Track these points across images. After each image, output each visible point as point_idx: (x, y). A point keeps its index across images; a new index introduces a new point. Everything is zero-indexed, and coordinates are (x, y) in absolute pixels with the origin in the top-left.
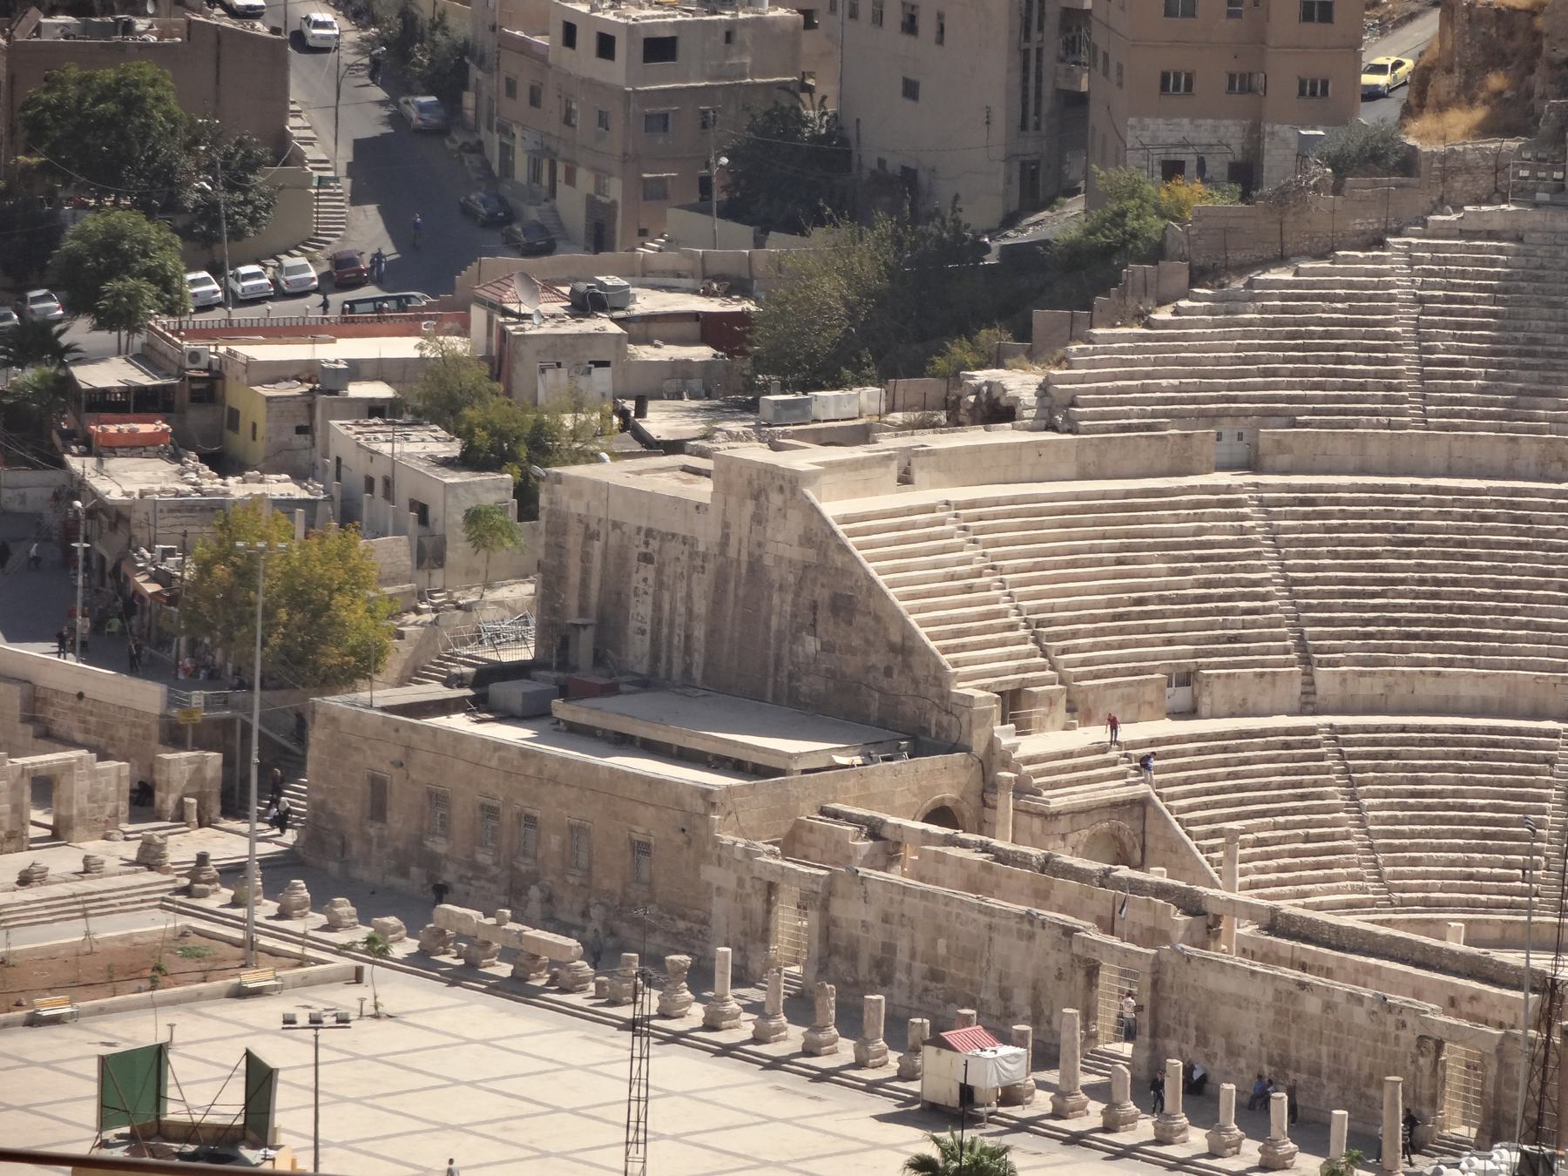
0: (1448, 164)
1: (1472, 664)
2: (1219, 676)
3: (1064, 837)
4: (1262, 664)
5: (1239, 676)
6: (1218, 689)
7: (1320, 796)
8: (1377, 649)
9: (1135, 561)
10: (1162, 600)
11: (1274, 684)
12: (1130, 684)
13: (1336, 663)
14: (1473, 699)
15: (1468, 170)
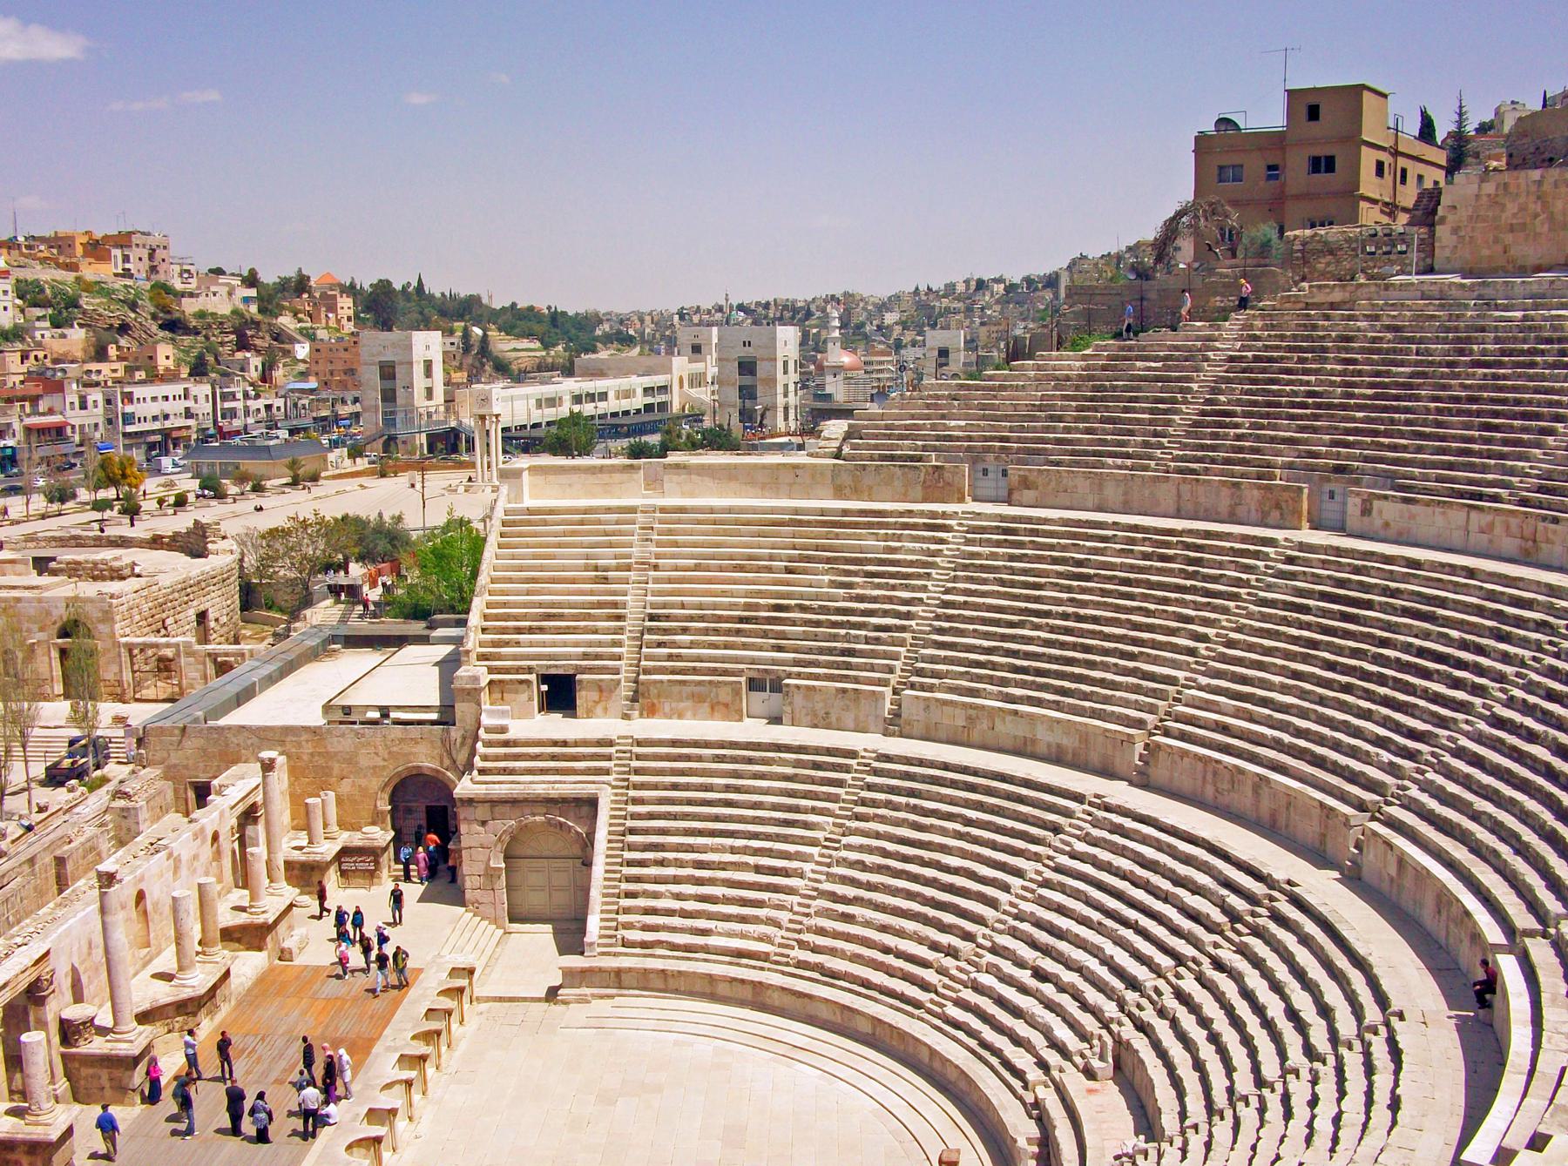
0: (1309, 247)
1: (1057, 706)
2: (798, 687)
3: (484, 823)
4: (856, 680)
5: (820, 689)
6: (798, 699)
7: (806, 826)
8: (979, 679)
9: (805, 572)
10: (803, 609)
11: (856, 700)
12: (700, 683)
13: (931, 688)
14: (1049, 746)
15: (1331, 253)
